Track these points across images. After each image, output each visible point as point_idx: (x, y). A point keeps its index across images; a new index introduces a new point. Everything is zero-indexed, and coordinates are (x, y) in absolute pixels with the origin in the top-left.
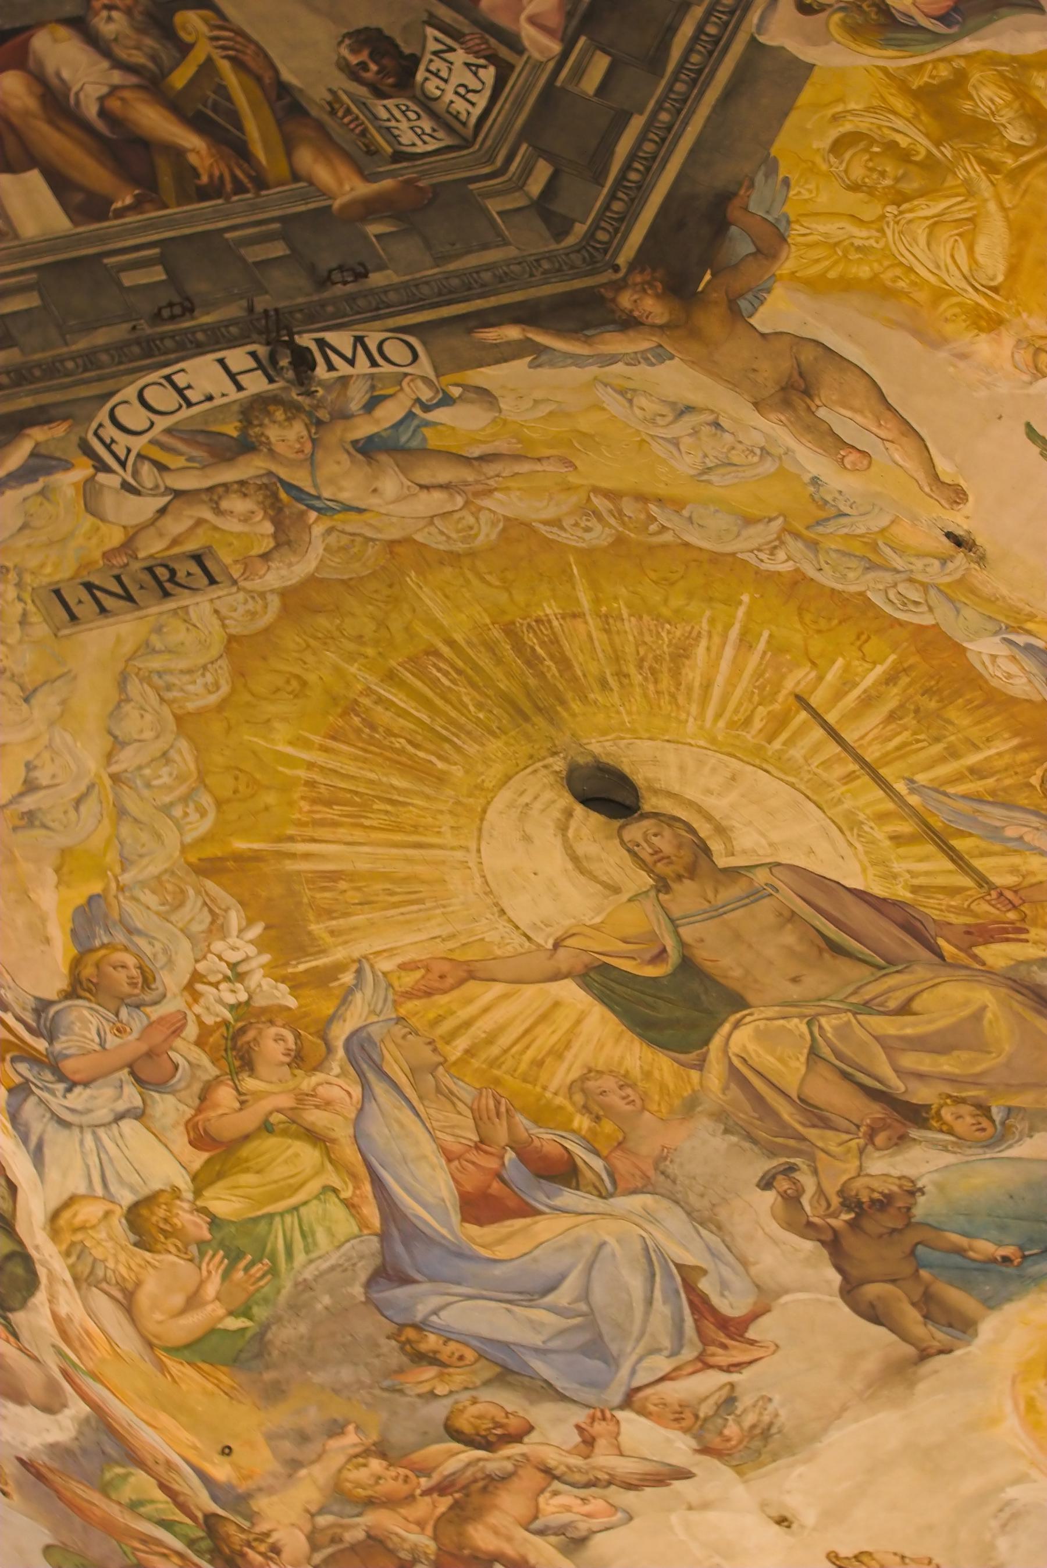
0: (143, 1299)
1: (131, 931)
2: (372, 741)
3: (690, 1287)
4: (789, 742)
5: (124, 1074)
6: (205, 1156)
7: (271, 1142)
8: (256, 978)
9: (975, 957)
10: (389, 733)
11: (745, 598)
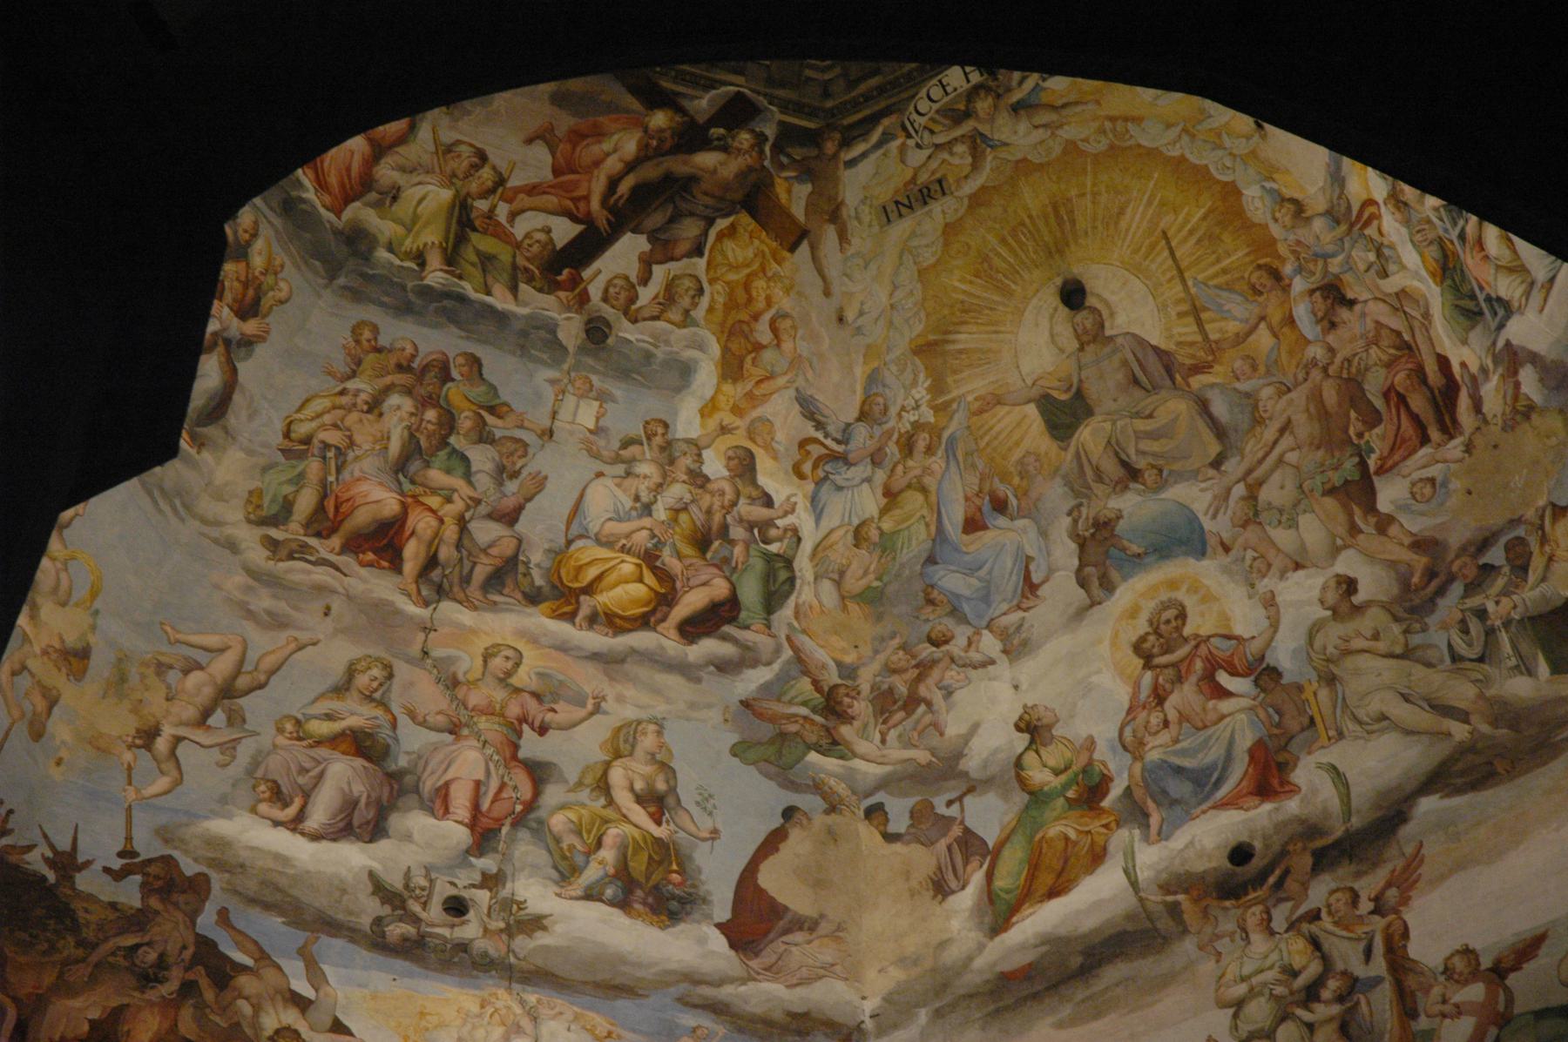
0: (849, 574)
1: (884, 386)
2: (991, 278)
3: (1027, 567)
4: (1153, 261)
5: (869, 460)
6: (885, 500)
7: (909, 493)
8: (924, 408)
9: (1188, 385)
10: (998, 272)
11: (1156, 175)
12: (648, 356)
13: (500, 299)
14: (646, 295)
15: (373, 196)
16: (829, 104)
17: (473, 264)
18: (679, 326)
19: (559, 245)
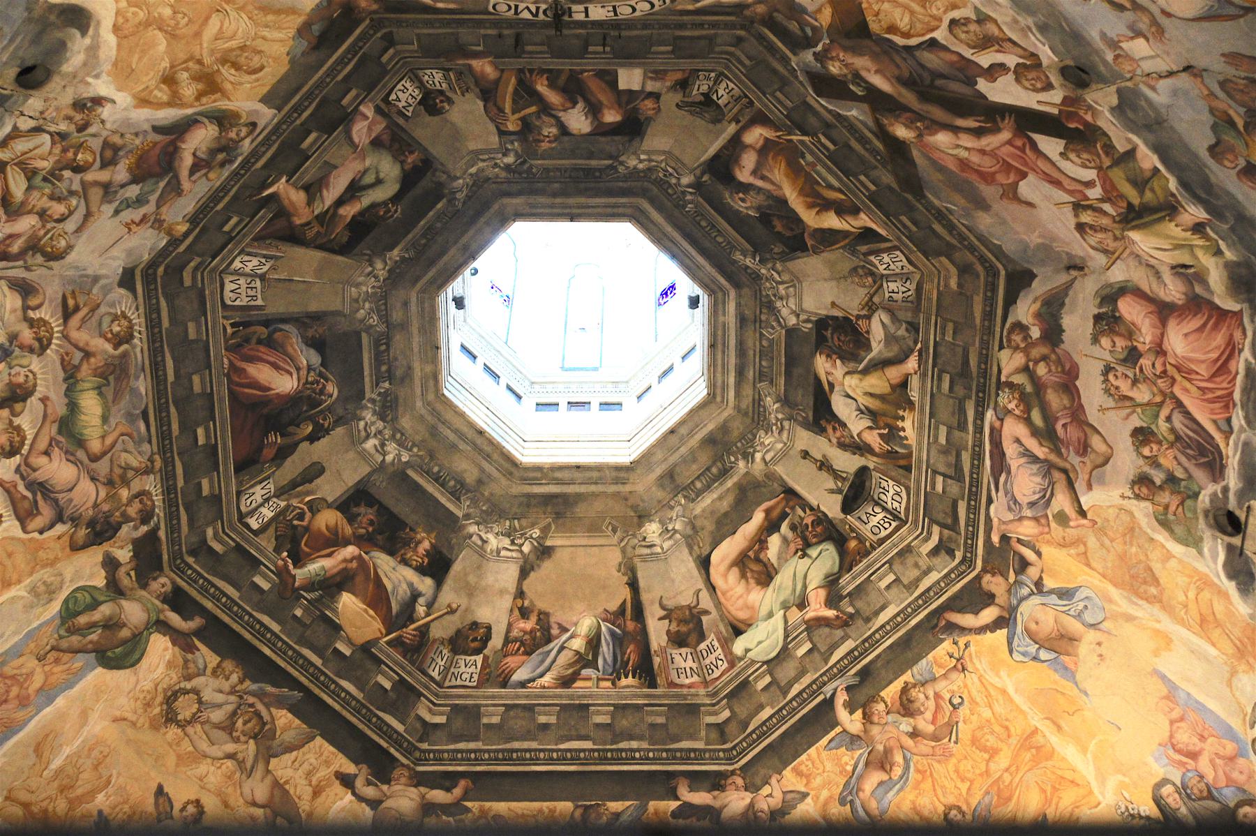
12: (1043, 29)
13: (1148, 159)
14: (1011, 60)
15: (1198, 289)
16: (742, 33)
17: (1152, 190)
18: (995, 21)
19: (1063, 142)
